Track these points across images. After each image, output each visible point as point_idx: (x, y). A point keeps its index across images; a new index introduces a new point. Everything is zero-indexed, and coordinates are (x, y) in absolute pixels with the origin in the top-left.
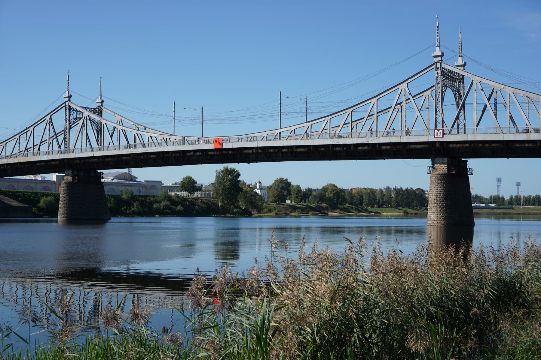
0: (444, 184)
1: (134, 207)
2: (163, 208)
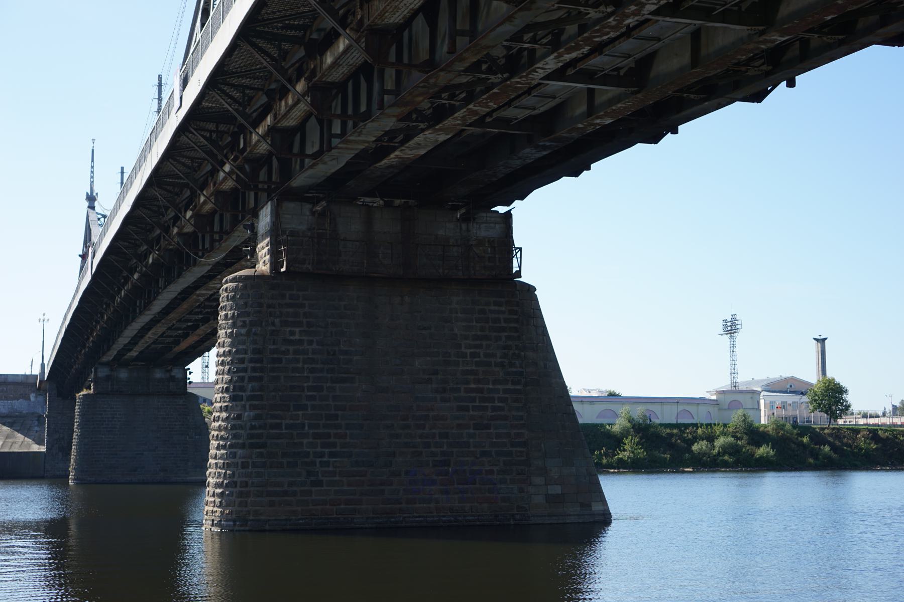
0: (234, 325)
1: (625, 450)
2: (719, 453)
